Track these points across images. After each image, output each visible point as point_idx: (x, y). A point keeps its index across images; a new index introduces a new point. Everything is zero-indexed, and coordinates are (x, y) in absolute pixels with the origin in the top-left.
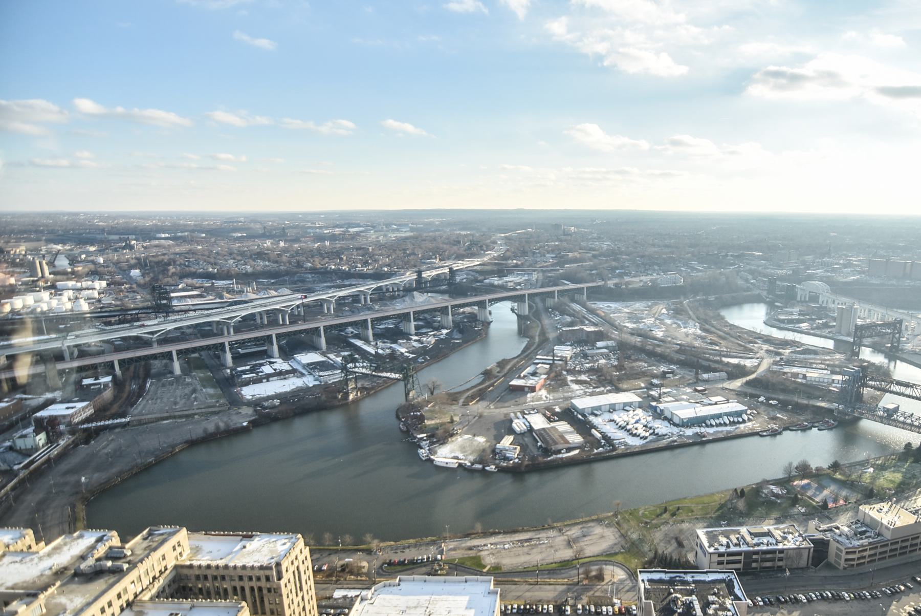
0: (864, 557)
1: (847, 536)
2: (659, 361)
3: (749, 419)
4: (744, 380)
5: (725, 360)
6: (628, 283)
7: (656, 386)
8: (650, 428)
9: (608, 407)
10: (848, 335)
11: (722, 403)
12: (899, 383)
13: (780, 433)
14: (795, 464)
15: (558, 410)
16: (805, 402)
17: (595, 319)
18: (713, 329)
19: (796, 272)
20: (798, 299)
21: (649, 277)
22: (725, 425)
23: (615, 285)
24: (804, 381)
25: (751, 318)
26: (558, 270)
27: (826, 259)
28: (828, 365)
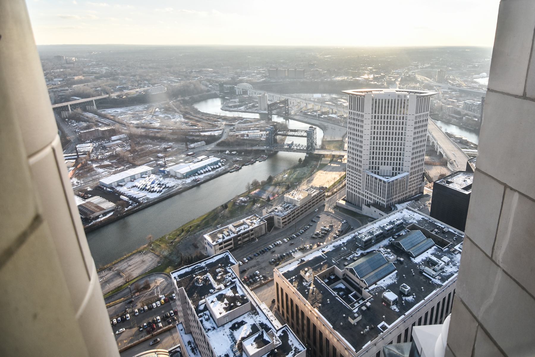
0: (290, 219)
1: (281, 211)
2: (160, 142)
3: (222, 165)
4: (216, 143)
5: (202, 134)
6: (127, 94)
7: (162, 158)
8: (163, 185)
9: (129, 179)
10: (265, 110)
11: (205, 159)
12: (292, 131)
13: (241, 168)
14: (251, 183)
15: (89, 189)
16: (250, 149)
17: (107, 121)
18: (191, 117)
19: (233, 78)
20: (237, 94)
21: (142, 89)
22: (210, 171)
23: (118, 96)
24: (248, 138)
25: (213, 107)
26: (67, 90)
27: (247, 71)
28: (258, 127)
